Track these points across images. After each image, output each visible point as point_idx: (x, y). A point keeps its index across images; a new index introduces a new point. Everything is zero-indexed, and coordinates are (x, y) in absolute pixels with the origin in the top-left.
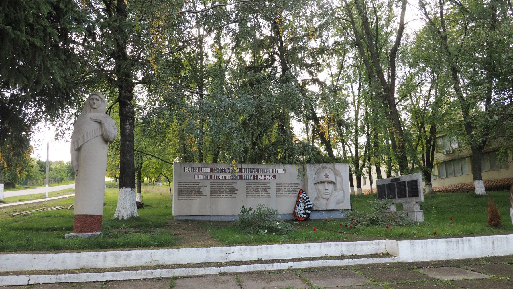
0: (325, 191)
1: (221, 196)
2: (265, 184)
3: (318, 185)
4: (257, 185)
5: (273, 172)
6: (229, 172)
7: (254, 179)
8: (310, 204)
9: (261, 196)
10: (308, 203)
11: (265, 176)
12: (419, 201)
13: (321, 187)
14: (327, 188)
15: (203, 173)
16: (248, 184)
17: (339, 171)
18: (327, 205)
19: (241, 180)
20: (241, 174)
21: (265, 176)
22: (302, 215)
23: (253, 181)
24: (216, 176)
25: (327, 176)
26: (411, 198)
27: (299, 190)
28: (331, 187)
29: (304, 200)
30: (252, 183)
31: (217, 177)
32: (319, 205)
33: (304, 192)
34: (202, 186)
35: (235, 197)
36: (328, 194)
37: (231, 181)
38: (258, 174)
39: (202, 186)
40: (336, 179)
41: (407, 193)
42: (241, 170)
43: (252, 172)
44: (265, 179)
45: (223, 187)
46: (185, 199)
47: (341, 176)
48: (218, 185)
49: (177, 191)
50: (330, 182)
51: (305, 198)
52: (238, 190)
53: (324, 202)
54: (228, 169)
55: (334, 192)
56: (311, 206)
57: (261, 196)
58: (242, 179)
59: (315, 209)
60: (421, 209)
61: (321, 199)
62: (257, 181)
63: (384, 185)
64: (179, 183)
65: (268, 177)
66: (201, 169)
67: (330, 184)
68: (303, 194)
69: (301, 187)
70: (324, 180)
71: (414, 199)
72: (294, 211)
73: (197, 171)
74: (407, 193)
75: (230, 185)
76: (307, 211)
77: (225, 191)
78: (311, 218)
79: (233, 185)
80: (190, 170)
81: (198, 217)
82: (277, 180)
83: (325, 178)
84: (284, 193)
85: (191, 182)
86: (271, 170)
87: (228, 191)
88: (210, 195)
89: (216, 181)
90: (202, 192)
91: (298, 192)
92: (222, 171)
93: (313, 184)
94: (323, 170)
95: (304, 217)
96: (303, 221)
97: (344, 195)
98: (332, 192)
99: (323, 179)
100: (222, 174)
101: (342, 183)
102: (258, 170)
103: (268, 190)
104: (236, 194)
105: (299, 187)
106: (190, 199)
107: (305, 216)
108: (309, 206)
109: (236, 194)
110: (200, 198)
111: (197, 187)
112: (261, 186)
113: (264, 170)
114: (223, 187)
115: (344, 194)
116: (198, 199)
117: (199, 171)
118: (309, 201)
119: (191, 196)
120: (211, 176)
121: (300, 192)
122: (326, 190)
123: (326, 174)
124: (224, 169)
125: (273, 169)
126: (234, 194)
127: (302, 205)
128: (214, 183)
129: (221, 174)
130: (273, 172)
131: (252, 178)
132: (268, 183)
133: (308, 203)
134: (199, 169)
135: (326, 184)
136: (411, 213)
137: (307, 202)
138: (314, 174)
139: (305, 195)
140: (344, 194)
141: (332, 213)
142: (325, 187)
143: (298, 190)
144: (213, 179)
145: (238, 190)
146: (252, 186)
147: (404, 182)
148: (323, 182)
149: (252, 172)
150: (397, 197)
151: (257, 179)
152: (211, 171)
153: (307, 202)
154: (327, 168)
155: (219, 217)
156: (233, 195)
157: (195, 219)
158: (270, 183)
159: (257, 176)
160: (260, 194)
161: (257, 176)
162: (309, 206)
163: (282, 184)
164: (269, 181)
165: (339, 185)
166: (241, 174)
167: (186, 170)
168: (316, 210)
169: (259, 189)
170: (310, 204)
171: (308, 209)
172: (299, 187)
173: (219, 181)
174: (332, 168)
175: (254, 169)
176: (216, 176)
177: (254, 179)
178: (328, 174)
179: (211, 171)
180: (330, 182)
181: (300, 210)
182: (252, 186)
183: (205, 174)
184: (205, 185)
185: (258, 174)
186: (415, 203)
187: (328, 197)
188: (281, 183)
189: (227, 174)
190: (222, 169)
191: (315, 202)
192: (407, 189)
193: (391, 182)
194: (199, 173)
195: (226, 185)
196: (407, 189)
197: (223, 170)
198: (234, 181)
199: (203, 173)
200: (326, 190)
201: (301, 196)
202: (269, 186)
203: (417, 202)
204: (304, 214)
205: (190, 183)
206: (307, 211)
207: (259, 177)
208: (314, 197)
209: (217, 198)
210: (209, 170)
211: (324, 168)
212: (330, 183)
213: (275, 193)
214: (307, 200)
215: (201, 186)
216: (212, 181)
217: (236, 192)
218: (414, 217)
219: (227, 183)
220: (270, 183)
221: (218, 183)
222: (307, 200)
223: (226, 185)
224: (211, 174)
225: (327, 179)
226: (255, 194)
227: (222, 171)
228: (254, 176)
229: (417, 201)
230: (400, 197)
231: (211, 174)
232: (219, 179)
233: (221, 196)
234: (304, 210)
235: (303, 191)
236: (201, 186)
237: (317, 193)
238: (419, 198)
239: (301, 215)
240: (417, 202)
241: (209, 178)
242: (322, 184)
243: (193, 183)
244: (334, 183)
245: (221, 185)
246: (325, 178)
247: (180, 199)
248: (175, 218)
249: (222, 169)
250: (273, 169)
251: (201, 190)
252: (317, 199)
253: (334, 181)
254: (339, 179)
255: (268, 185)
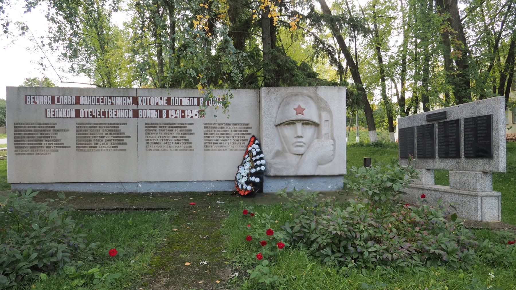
0: (296, 140)
1: (98, 148)
2: (182, 126)
3: (282, 127)
4: (168, 127)
5: (198, 104)
6: (112, 104)
7: (161, 116)
8: (260, 165)
9: (175, 148)
10: (258, 163)
11: (183, 111)
12: (492, 169)
13: (288, 131)
14: (300, 134)
15: (61, 107)
16: (150, 126)
17: (326, 102)
18: (298, 167)
19: (135, 119)
20: (135, 107)
21: (183, 111)
22: (245, 186)
23: (160, 120)
24: (86, 110)
25: (300, 110)
26: (470, 161)
27: (251, 136)
28: (309, 131)
29: (253, 156)
30: (158, 124)
31: (90, 113)
32: (280, 167)
33: (257, 142)
34: (61, 130)
35: (125, 150)
36: (301, 146)
37: (116, 121)
38: (168, 108)
39: (61, 130)
40: (320, 117)
41: (463, 143)
42: (135, 100)
43: (157, 104)
44: (183, 116)
45: (101, 132)
46: (28, 154)
47: (330, 112)
48: (92, 127)
49: (14, 139)
50: (307, 123)
51: (254, 153)
52: (129, 137)
53: (293, 159)
54: (110, 98)
55: (316, 141)
56: (263, 168)
57: (175, 148)
58: (137, 117)
59: (272, 173)
60: (494, 189)
61: (288, 154)
62: (167, 121)
63: (412, 128)
64: (17, 124)
65: (188, 113)
66: (58, 99)
67: (308, 127)
68: (254, 145)
69: (253, 132)
70: (294, 118)
71: (479, 164)
72: (236, 178)
73: (50, 102)
74: (463, 143)
75: (114, 127)
76: (253, 179)
77: (104, 139)
78: (265, 190)
79: (121, 127)
80: (38, 101)
81: (56, 185)
82: (209, 118)
83: (297, 114)
84: (220, 142)
85: (39, 122)
86: (196, 100)
87: (111, 138)
88: (75, 145)
89: (86, 120)
90: (60, 140)
91: (246, 140)
92: (98, 102)
93: (273, 125)
94: (294, 98)
95: (246, 190)
96: (245, 196)
97: (334, 150)
98: (311, 141)
99: (293, 115)
100: (99, 107)
101: (332, 124)
102: (169, 100)
103: (188, 137)
104: (126, 144)
105: (249, 131)
106: (39, 154)
107: (249, 188)
108: (258, 169)
109: (126, 144)
110: (57, 151)
111: (52, 132)
112: (174, 129)
113: (181, 100)
114: (101, 132)
115: (334, 145)
116: (53, 154)
117: (53, 102)
118: (261, 159)
119: (40, 147)
120: (77, 112)
121: (250, 141)
122: (298, 137)
123: (299, 106)
124: (102, 99)
125: (198, 99)
126: (123, 144)
127: (248, 165)
128: (83, 124)
129: (96, 107)
130: (198, 104)
131: (157, 114)
132: (189, 124)
133: (258, 163)
134: (53, 98)
135: (299, 125)
136: (469, 198)
137: (256, 160)
138: (276, 107)
139: (257, 146)
140: (334, 145)
141: (309, 181)
142: (296, 132)
143: (248, 137)
144: (82, 116)
145: (129, 137)
146: (158, 129)
147: (457, 122)
148: (292, 123)
149: (157, 104)
150: (437, 156)
151: (167, 116)
152: (78, 101)
153: (256, 160)
154: (302, 94)
155: (95, 185)
156: (120, 147)
157: (51, 189)
158: (192, 124)
159: (167, 111)
160: (173, 145)
161: (167, 111)
162: (258, 169)
163: (217, 126)
164: (190, 121)
165: (325, 129)
166: (135, 107)
167: (28, 100)
168: (276, 177)
169: (171, 136)
170: (260, 165)
171: (256, 174)
172: (249, 131)
173: (92, 121)
174: (312, 95)
175: (161, 98)
176: (86, 110)
177: (161, 116)
178: (303, 106)
179: (78, 101)
180: (307, 123)
181: (243, 176)
182: (158, 129)
183: (65, 107)
184: (66, 128)
185: (168, 108)
186: (480, 174)
187: (301, 150)
188: (214, 124)
189: (108, 107)
190: (98, 99)
191: (272, 161)
192: (462, 138)
193: (428, 121)
194: (54, 106)
195: (107, 127)
196: (462, 138)
197: (101, 101)
198: (121, 121)
199: (61, 107)
200: (298, 137)
201: (250, 149)
202: (190, 130)
203: (485, 173)
204: (248, 183)
205: (37, 124)
206: (253, 179)
207: (172, 113)
208: (274, 152)
209: (89, 151)
210: (74, 101)
211: (296, 95)
212: (307, 124)
213: (203, 142)
214: (258, 157)
215: (59, 131)
216: (78, 120)
217: (126, 140)
218: (476, 209)
219: (109, 124)
220: (192, 124)
221: (90, 124)
222: (258, 157)
223: (107, 127)
224: (78, 107)
225: (300, 117)
226: (163, 145)
227: (98, 102)
228: (161, 111)
229: (487, 168)
230: (445, 155)
231: (78, 107)
232: (93, 116)
233: (98, 148)
234: (248, 175)
235: (256, 139)
236: (59, 131)
237: (282, 143)
238: (493, 162)
239: (242, 186)
240: (485, 173)
241: (73, 114)
242: (292, 126)
243: (43, 124)
244: (316, 125)
245: (98, 129)
246: (297, 114)
247: (19, 154)
248: (13, 187)
249: (98, 99)
250: (198, 99)
251: (58, 137)
252: (278, 154)
253: (316, 120)
254: (325, 115)
255: (189, 127)
